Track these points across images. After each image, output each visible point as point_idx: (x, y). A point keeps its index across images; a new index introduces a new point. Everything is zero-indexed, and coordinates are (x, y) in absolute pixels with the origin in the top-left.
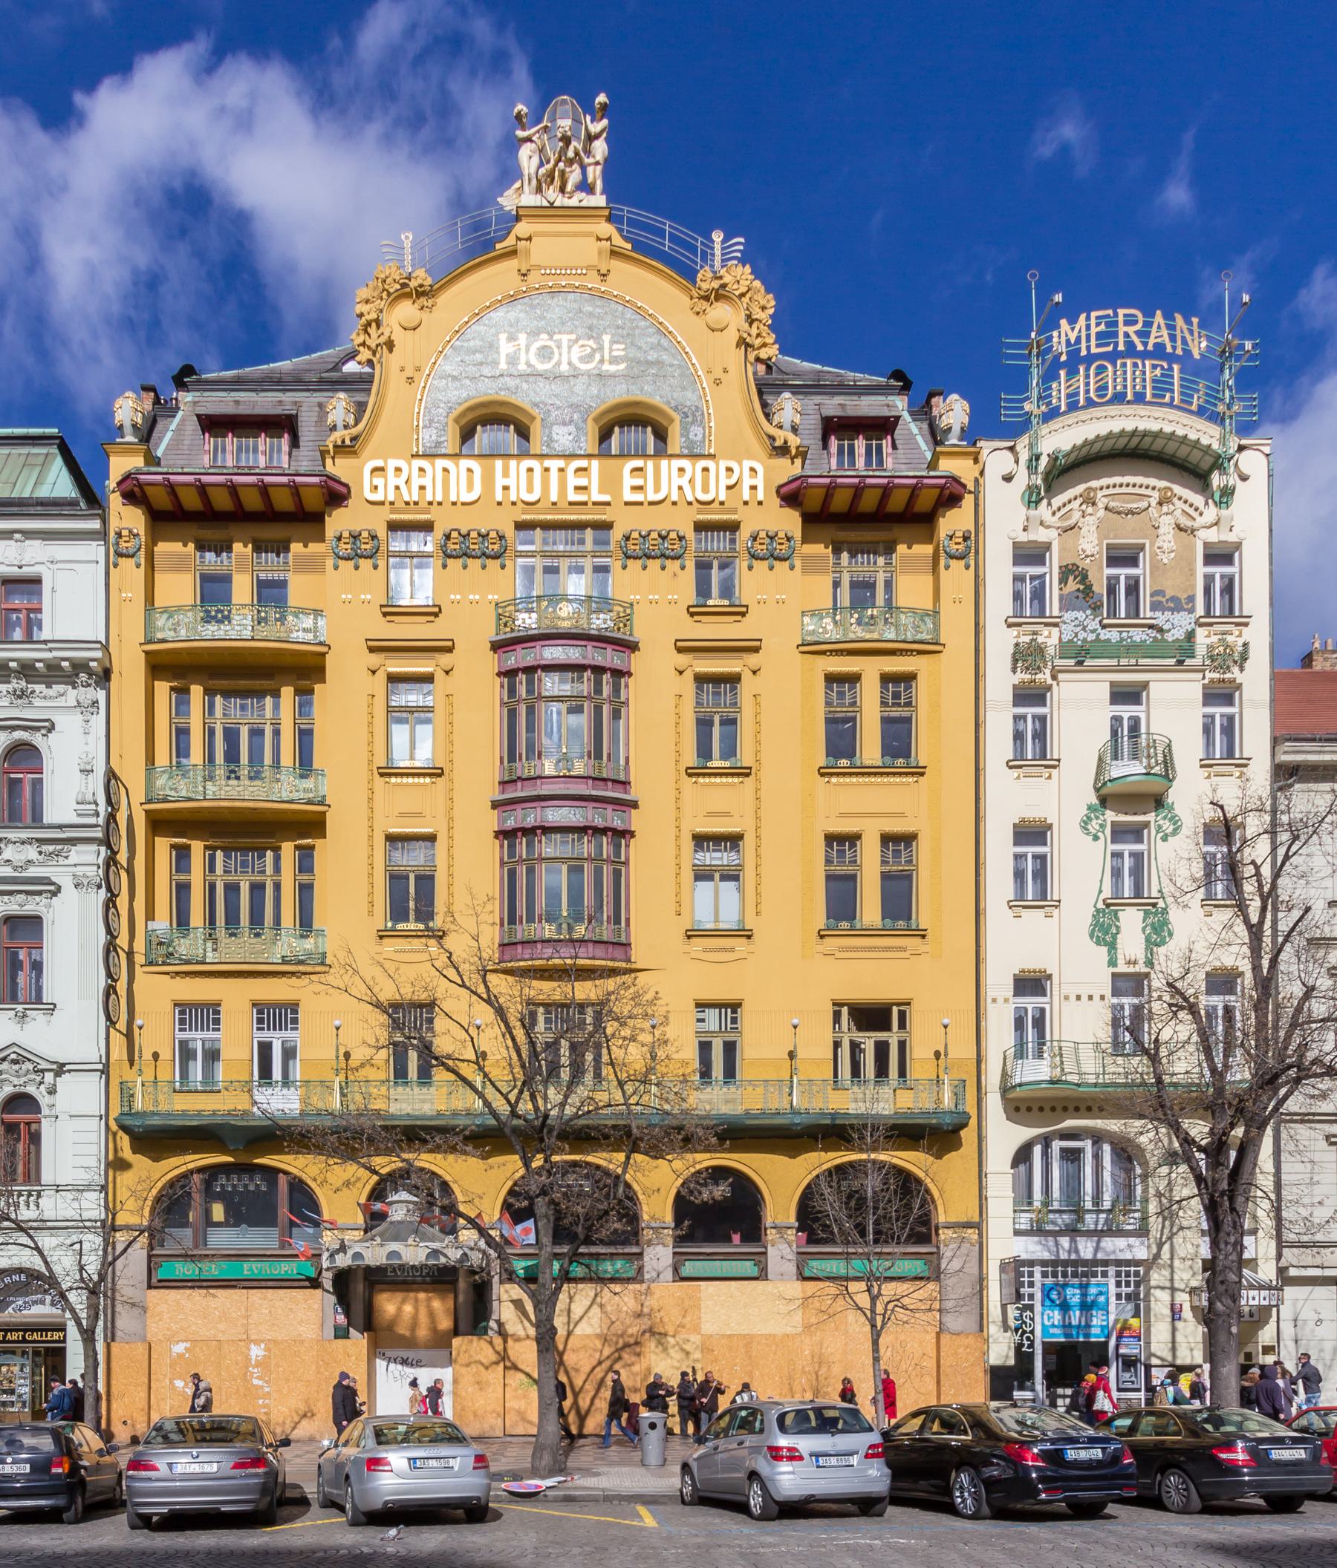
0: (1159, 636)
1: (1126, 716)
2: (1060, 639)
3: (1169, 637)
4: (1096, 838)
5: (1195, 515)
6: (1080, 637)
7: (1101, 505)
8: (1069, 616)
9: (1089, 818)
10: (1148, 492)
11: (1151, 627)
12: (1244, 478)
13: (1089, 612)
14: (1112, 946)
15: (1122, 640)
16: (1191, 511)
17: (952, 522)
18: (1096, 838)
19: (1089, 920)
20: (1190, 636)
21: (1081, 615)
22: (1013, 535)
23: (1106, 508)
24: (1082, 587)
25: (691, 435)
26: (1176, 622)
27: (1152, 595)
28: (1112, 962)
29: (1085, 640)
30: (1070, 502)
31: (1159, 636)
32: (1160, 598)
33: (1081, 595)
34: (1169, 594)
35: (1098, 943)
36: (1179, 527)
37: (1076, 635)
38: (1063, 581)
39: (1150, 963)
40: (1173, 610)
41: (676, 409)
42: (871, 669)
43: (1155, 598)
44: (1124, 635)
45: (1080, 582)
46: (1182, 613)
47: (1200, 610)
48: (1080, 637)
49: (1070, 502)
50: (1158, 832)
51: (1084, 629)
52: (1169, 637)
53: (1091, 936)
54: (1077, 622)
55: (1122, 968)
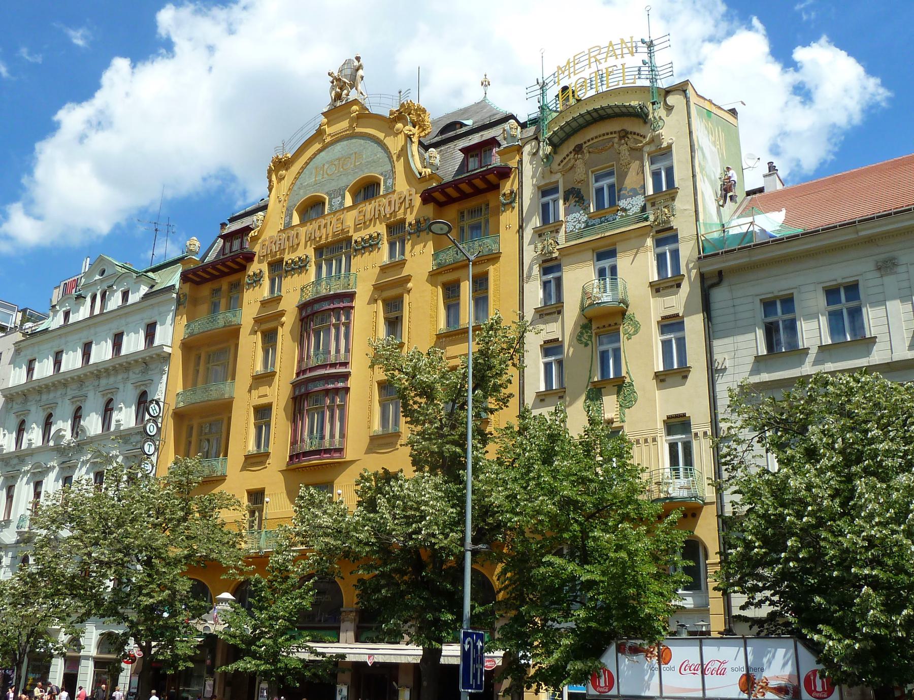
0: (624, 214)
2: (566, 231)
4: (586, 345)
5: (641, 139)
6: (577, 227)
7: (585, 151)
8: (570, 218)
10: (614, 135)
13: (581, 212)
17: (508, 187)
18: (586, 345)
21: (577, 215)
25: (388, 184)
26: (634, 203)
29: (580, 228)
30: (568, 155)
36: (632, 149)
37: (575, 226)
40: (631, 197)
41: (382, 174)
45: (576, 197)
47: (650, 191)
48: (577, 227)
49: (568, 155)
51: (579, 223)
52: (630, 213)
54: (575, 219)
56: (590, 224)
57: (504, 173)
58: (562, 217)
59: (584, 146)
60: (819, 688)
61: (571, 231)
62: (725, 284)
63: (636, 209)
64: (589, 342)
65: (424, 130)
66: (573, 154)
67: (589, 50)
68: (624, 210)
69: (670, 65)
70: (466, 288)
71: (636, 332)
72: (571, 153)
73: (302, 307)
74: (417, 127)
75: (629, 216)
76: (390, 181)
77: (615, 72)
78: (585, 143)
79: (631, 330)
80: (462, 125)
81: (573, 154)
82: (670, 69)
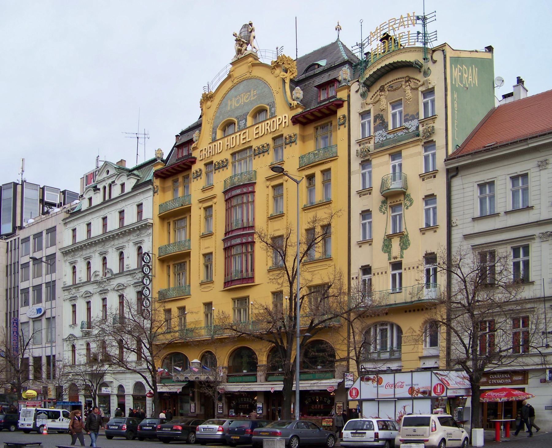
0: (407, 131)
1: (397, 164)
2: (374, 142)
3: (410, 131)
4: (384, 213)
5: (418, 82)
6: (381, 140)
7: (386, 90)
8: (377, 133)
9: (382, 206)
10: (402, 80)
11: (404, 129)
12: (435, 62)
13: (383, 130)
14: (389, 253)
15: (395, 136)
16: (416, 81)
17: (342, 112)
18: (384, 213)
19: (382, 244)
20: (418, 128)
21: (381, 132)
22: (358, 111)
23: (388, 91)
24: (381, 121)
25: (272, 111)
26: (413, 124)
27: (404, 117)
28: (389, 259)
29: (382, 141)
30: (376, 93)
31: (407, 131)
32: (407, 117)
33: (381, 124)
34: (410, 114)
35: (385, 253)
37: (379, 139)
38: (375, 121)
39: (402, 257)
40: (411, 120)
41: (268, 105)
42: (317, 171)
43: (405, 118)
44: (395, 134)
45: (381, 120)
46: (415, 120)
47: (422, 116)
48: (381, 140)
49: (376, 93)
50: (405, 206)
51: (382, 137)
52: (410, 131)
53: (383, 250)
55: (392, 260)
56: (388, 138)
57: (339, 104)
58: (372, 134)
59: (385, 87)
60: (439, 391)
61: (378, 142)
62: (459, 175)
63: (414, 128)
64: (386, 212)
65: (293, 74)
66: (379, 92)
67: (389, 21)
68: (407, 129)
69: (435, 33)
70: (319, 179)
71: (411, 205)
72: (378, 91)
73: (225, 192)
74: (289, 71)
75: (410, 133)
76: (273, 109)
77: (404, 37)
78: (386, 84)
79: (408, 203)
80: (319, 66)
81: (379, 92)
82: (435, 36)
